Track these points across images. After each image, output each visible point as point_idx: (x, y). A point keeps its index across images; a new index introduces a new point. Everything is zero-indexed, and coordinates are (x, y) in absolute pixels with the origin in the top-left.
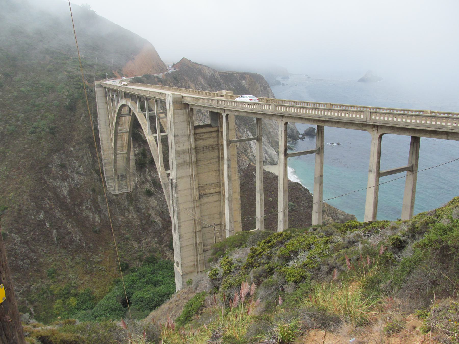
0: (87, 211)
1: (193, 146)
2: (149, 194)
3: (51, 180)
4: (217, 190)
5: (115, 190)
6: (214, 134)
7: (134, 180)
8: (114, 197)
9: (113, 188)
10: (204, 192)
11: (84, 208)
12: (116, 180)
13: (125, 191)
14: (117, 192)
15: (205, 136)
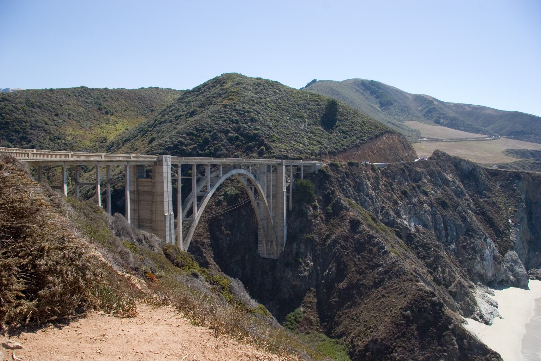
0: (234, 264)
1: (135, 189)
2: (287, 265)
3: (218, 233)
4: (150, 225)
5: (264, 254)
6: (150, 184)
7: (281, 250)
8: (262, 259)
9: (262, 252)
10: (142, 224)
11: (233, 261)
12: (265, 245)
13: (272, 257)
14: (265, 256)
15: (144, 184)
